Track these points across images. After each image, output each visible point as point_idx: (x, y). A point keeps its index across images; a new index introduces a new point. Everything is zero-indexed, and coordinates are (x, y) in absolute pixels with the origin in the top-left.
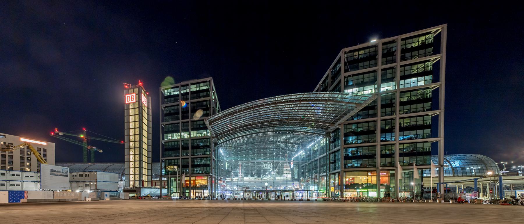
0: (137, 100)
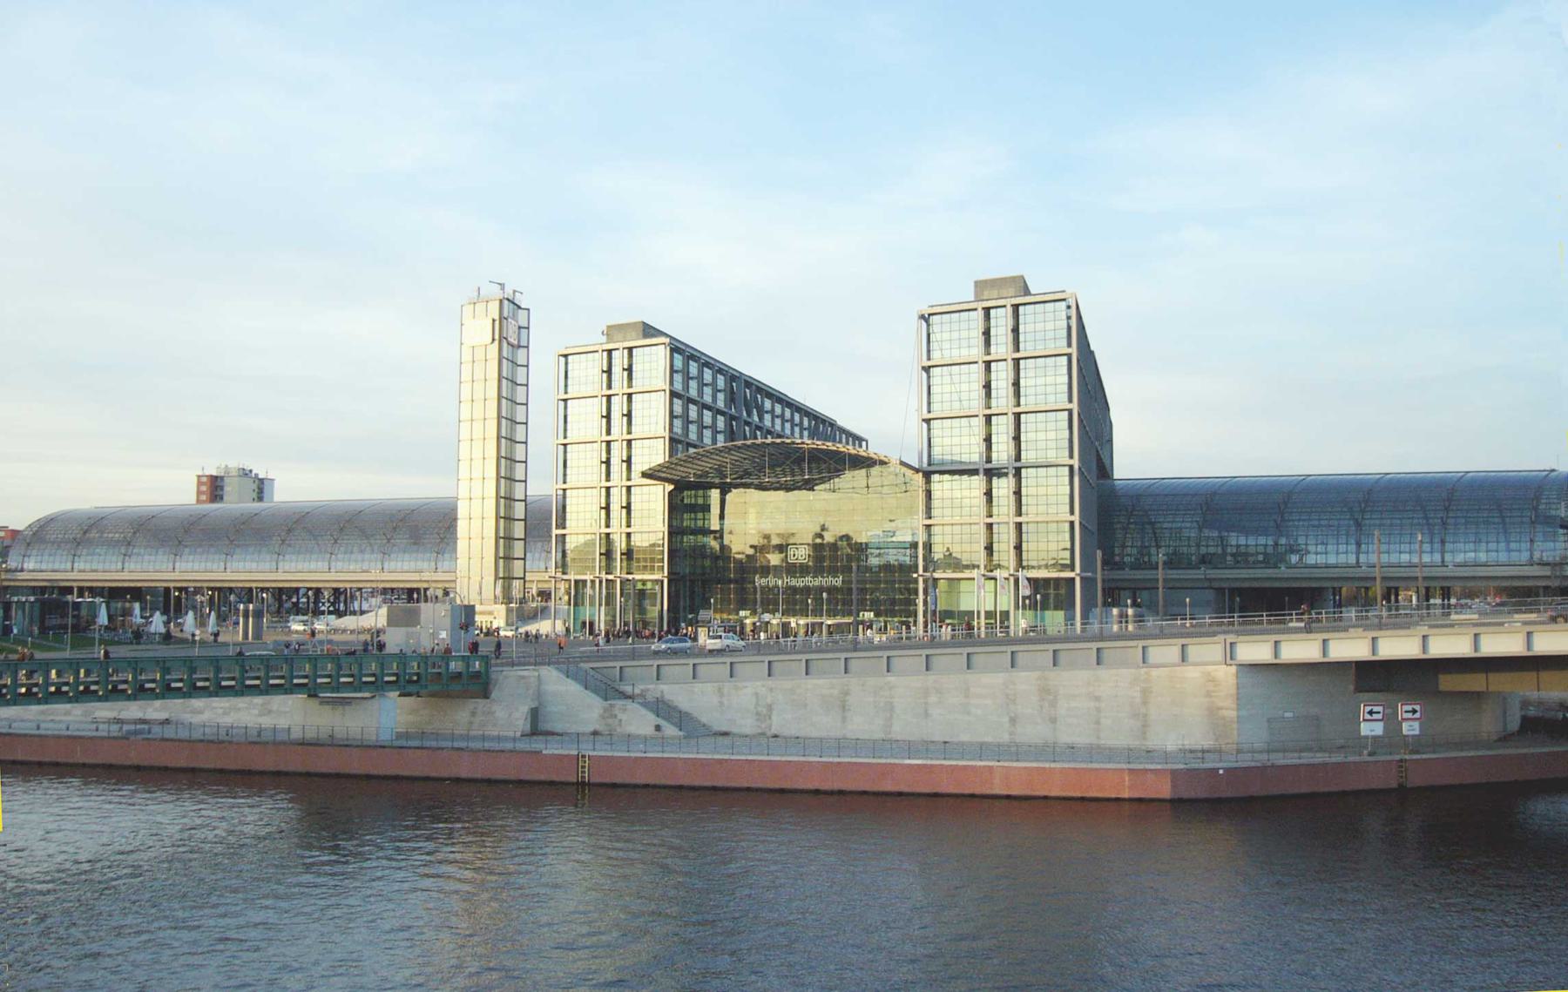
0: (497, 337)
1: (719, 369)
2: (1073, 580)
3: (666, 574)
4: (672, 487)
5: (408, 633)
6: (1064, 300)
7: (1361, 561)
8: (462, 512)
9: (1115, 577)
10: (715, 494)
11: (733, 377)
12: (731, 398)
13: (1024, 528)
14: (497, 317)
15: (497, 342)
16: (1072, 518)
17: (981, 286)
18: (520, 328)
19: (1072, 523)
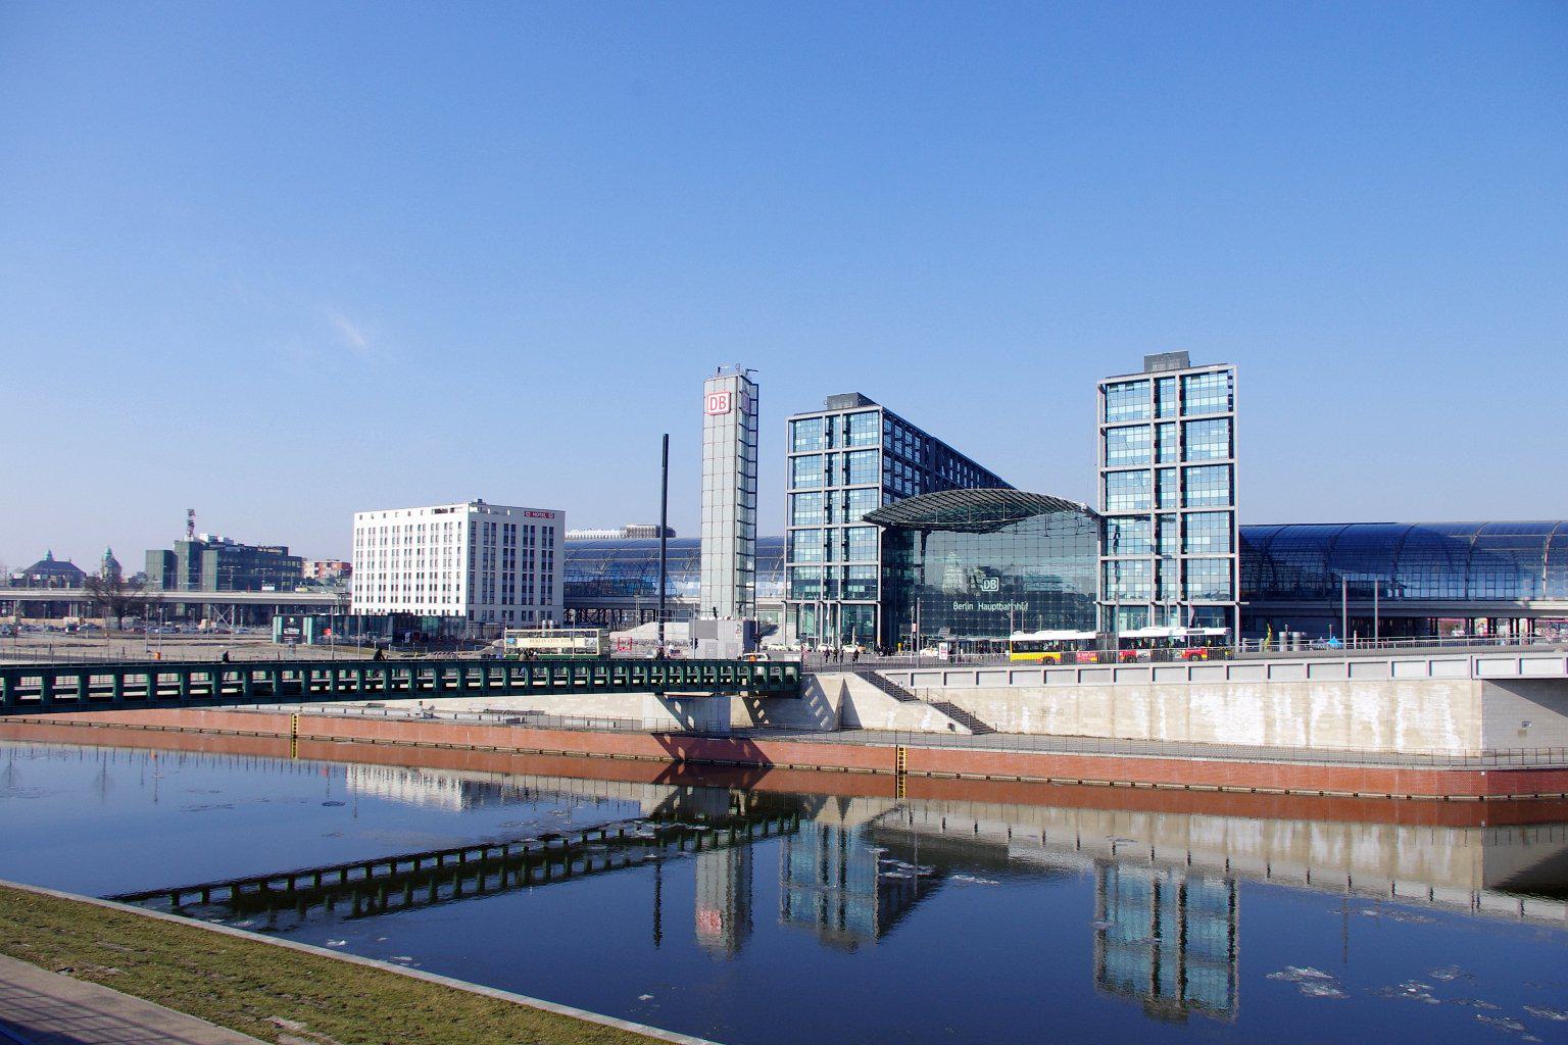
0: (733, 406)
1: (917, 433)
2: (1233, 607)
3: (879, 600)
4: (884, 529)
5: (707, 643)
6: (1226, 371)
7: (1469, 595)
8: (705, 548)
9: (1303, 607)
10: (917, 535)
11: (927, 439)
12: (925, 457)
13: (1189, 564)
14: (733, 391)
15: (733, 412)
16: (1232, 556)
17: (1149, 361)
18: (751, 400)
19: (1232, 561)
